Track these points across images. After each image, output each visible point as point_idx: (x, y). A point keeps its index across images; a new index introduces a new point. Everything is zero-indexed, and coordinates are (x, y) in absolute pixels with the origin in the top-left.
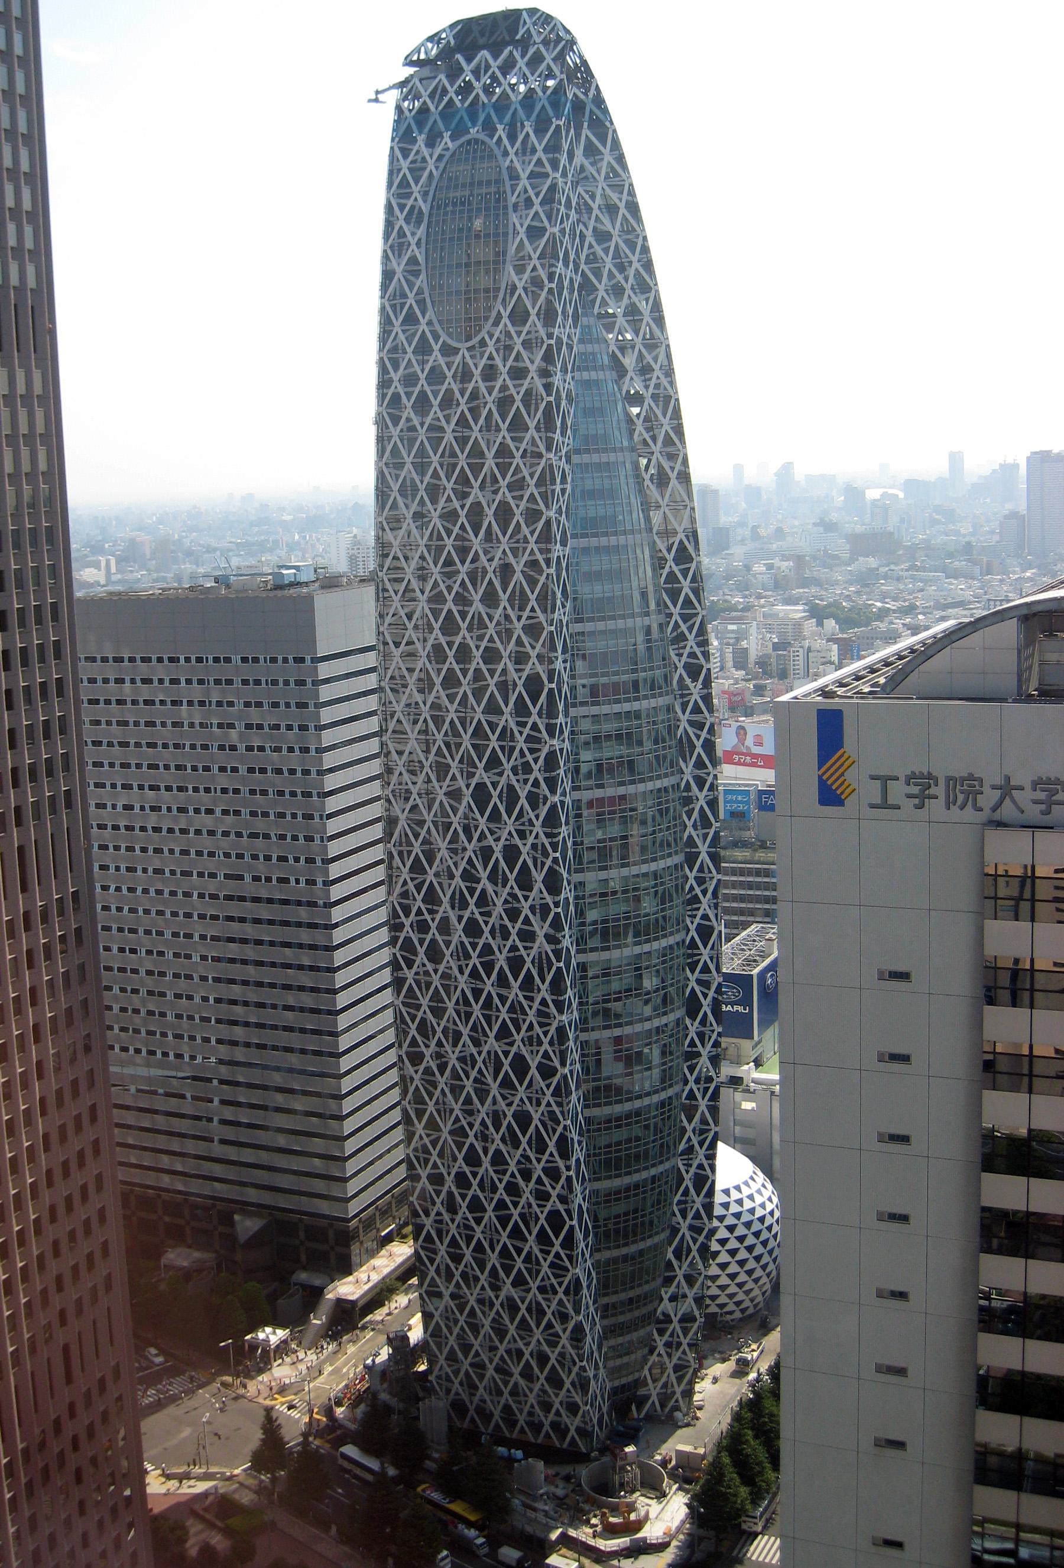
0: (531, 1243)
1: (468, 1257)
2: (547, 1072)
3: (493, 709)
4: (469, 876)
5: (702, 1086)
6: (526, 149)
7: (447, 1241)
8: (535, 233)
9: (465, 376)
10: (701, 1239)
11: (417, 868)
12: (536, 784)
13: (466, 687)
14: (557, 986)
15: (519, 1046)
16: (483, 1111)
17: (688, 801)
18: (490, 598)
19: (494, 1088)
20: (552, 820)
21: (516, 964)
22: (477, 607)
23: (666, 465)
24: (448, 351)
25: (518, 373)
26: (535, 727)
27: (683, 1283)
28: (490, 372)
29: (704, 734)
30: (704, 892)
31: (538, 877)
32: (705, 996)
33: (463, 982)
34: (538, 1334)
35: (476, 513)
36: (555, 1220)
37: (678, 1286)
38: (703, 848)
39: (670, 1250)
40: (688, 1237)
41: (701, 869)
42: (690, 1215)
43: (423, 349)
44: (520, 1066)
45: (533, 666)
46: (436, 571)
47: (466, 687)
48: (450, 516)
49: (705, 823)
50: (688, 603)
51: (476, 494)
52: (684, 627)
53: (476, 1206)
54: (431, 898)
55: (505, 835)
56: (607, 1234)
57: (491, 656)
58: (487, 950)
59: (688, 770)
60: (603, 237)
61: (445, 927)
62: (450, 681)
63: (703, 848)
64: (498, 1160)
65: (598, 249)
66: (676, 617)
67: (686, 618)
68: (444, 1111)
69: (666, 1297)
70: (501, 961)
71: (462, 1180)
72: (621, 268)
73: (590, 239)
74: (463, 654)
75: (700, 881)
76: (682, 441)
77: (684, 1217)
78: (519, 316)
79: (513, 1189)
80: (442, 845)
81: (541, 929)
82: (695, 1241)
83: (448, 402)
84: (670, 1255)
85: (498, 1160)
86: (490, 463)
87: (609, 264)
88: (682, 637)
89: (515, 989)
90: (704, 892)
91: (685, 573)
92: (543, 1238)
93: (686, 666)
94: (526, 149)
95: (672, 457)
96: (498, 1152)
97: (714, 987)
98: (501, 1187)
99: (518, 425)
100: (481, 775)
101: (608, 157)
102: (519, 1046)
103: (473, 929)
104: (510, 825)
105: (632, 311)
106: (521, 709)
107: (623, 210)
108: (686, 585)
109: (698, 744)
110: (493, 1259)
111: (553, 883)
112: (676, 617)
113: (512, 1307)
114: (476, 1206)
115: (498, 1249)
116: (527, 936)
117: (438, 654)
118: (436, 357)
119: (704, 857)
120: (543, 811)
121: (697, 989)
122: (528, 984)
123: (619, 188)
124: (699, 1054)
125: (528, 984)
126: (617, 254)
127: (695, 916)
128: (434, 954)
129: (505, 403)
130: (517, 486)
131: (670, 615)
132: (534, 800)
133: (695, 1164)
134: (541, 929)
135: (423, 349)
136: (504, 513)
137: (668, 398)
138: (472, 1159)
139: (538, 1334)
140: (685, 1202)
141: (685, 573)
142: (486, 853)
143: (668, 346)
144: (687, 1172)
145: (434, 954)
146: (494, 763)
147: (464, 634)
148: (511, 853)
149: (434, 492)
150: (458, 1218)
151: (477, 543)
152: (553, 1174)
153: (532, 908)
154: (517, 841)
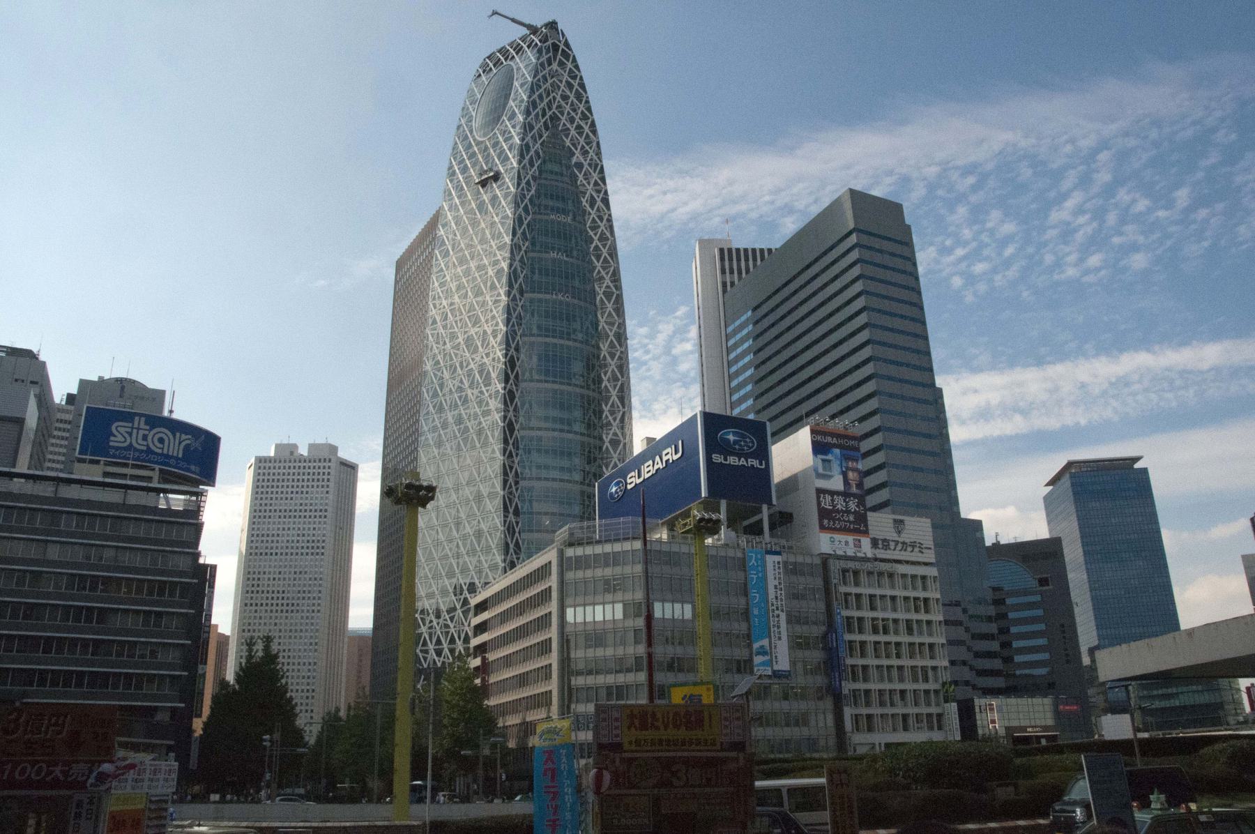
1: (446, 651)
4: (460, 389)
7: (434, 641)
12: (497, 324)
17: (606, 366)
23: (595, 194)
24: (478, 143)
26: (499, 295)
29: (615, 328)
30: (615, 419)
31: (494, 375)
38: (614, 393)
41: (613, 405)
49: (616, 379)
50: (605, 260)
52: (603, 273)
55: (478, 359)
58: (466, 429)
60: (565, 98)
63: (614, 393)
65: (563, 103)
66: (599, 268)
67: (604, 268)
72: (574, 110)
73: (558, 98)
75: (612, 413)
76: (605, 184)
80: (446, 375)
87: (568, 108)
88: (602, 278)
90: (615, 419)
91: (604, 246)
93: (604, 293)
95: (599, 192)
96: (465, 562)
98: (465, 588)
101: (569, 65)
103: (459, 421)
105: (579, 127)
107: (576, 86)
108: (605, 252)
109: (611, 334)
112: (599, 268)
115: (463, 636)
119: (614, 398)
120: (500, 337)
123: (574, 78)
126: (572, 104)
128: (439, 444)
131: (595, 268)
137: (597, 165)
141: (604, 246)
142: (470, 374)
143: (598, 143)
150: (441, 621)
153: (490, 396)
154: (485, 360)
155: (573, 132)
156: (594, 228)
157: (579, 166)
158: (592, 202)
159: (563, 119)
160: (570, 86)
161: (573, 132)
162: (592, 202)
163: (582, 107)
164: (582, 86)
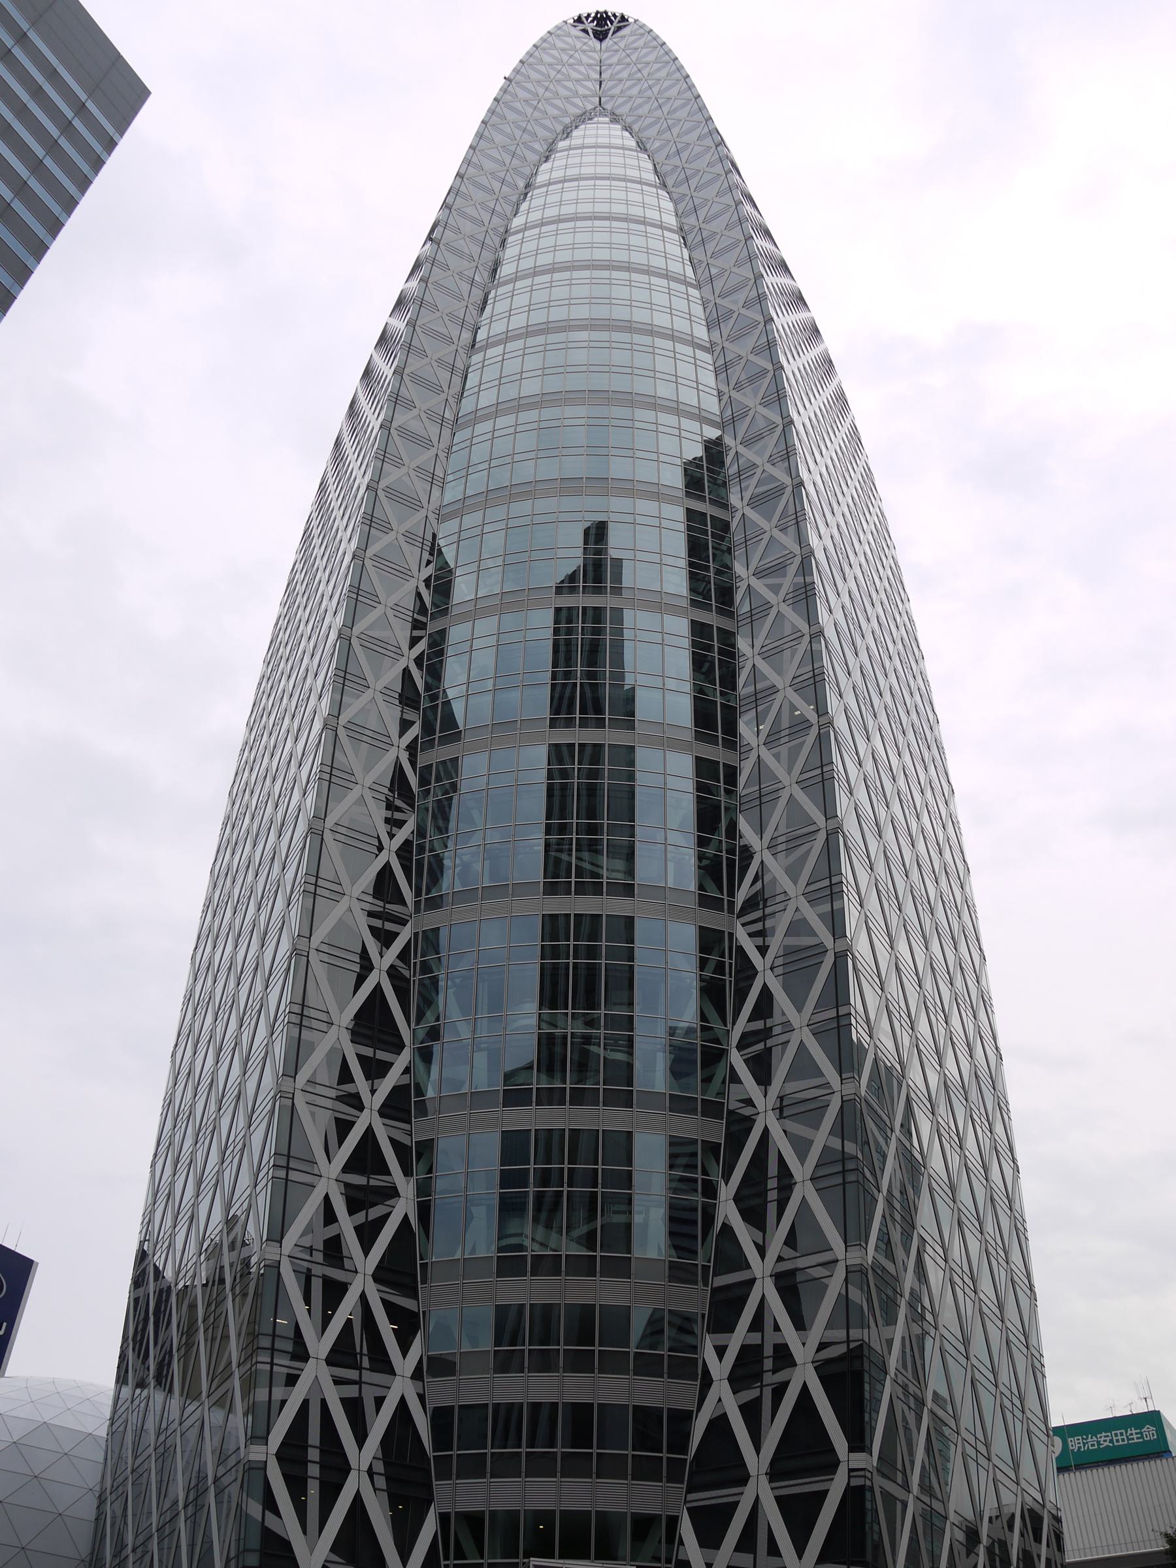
5: (784, 750)
10: (822, 1137)
27: (777, 1307)
32: (775, 589)
37: (757, 1324)
39: (727, 1192)
40: (781, 1143)
42: (781, 1069)
69: (719, 1370)
77: (763, 1077)
82: (802, 1147)
84: (728, 1211)
97: (792, 569)
121: (756, 584)
124: (773, 690)
127: (747, 488)
133: (780, 924)
140: (767, 1033)
144: (763, 950)
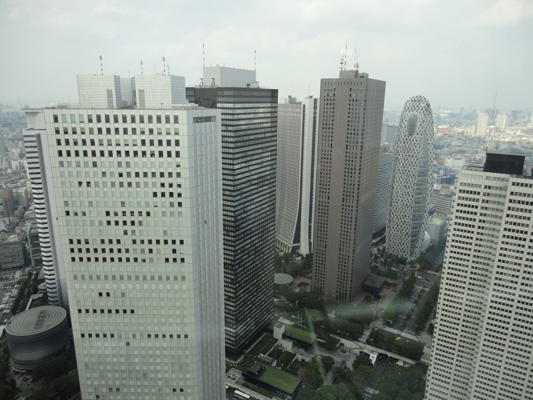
0: (404, 236)
2: (409, 217)
3: (408, 177)
6: (421, 115)
8: (421, 125)
9: (410, 140)
11: (396, 193)
13: (405, 174)
14: (411, 208)
15: (406, 214)
16: (400, 220)
18: (410, 165)
19: (402, 218)
20: (413, 190)
21: (407, 205)
22: (408, 166)
25: (417, 141)
28: (413, 140)
33: (400, 206)
34: (403, 246)
35: (409, 156)
36: (407, 233)
43: (405, 136)
44: (406, 216)
45: (414, 173)
46: (403, 161)
47: (405, 174)
48: (406, 155)
51: (409, 153)
53: (398, 231)
54: (398, 197)
56: (413, 236)
57: (409, 171)
59: (429, 185)
60: (428, 125)
61: (399, 200)
62: (403, 173)
64: (401, 226)
68: (395, 220)
70: (405, 204)
71: (396, 228)
74: (405, 171)
78: (418, 134)
79: (402, 230)
80: (400, 191)
81: (410, 201)
83: (407, 143)
85: (401, 226)
86: (412, 150)
89: (406, 208)
92: (405, 235)
94: (421, 115)
99: (416, 147)
100: (406, 184)
101: (430, 116)
102: (406, 214)
103: (402, 200)
104: (408, 189)
106: (412, 177)
110: (399, 237)
111: (413, 196)
113: (400, 243)
114: (398, 231)
116: (409, 202)
117: (402, 170)
118: (407, 137)
122: (408, 207)
125: (408, 207)
128: (397, 203)
129: (415, 144)
130: (415, 153)
132: (412, 187)
134: (410, 201)
135: (405, 136)
136: (413, 156)
138: (398, 226)
139: (403, 246)
142: (405, 192)
145: (397, 203)
146: (407, 183)
147: (406, 168)
148: (408, 193)
149: (404, 152)
151: (409, 159)
152: (408, 228)
155: (429, 135)
156: (430, 159)
157: (429, 144)
158: (431, 153)
159: (427, 131)
160: (430, 122)
161: (429, 135)
162: (431, 153)
163: (432, 128)
164: (432, 122)
